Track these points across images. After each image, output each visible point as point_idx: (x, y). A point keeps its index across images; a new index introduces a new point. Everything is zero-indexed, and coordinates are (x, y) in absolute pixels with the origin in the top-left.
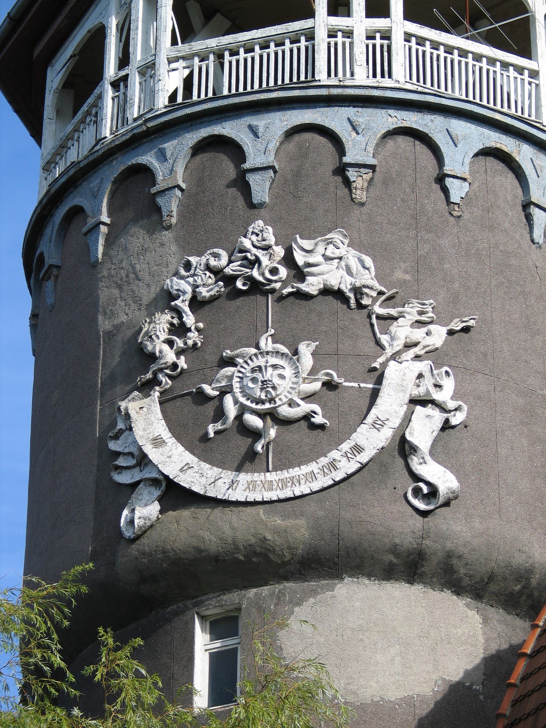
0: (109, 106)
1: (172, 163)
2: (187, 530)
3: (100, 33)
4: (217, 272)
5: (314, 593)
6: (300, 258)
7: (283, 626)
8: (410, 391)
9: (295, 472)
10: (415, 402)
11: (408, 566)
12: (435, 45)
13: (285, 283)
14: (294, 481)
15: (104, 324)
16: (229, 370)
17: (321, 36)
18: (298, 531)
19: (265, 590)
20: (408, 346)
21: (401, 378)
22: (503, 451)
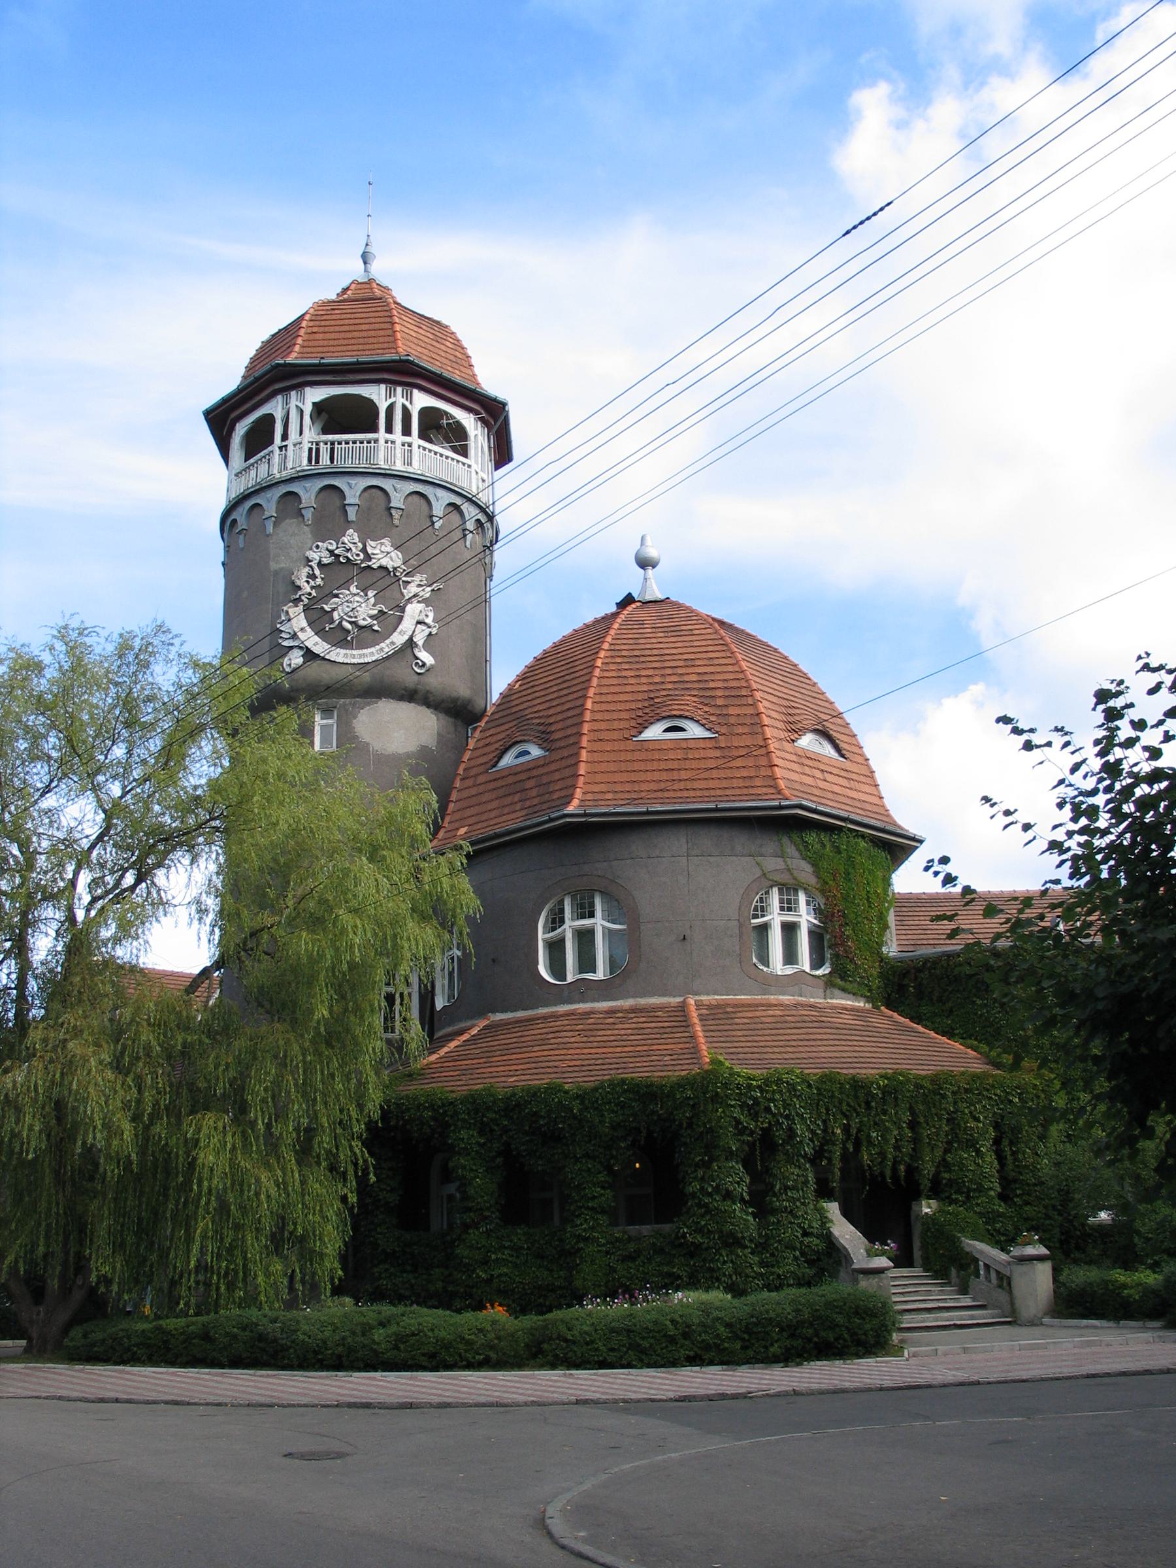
0: (276, 458)
1: (308, 493)
2: (315, 671)
3: (269, 419)
4: (331, 552)
5: (369, 704)
6: (370, 550)
7: (355, 717)
8: (418, 618)
9: (365, 651)
10: (419, 623)
11: (410, 695)
12: (430, 451)
13: (362, 561)
14: (365, 655)
15: (274, 566)
16: (336, 600)
17: (382, 442)
18: (366, 677)
19: (348, 701)
20: (415, 596)
21: (414, 610)
22: (451, 646)
